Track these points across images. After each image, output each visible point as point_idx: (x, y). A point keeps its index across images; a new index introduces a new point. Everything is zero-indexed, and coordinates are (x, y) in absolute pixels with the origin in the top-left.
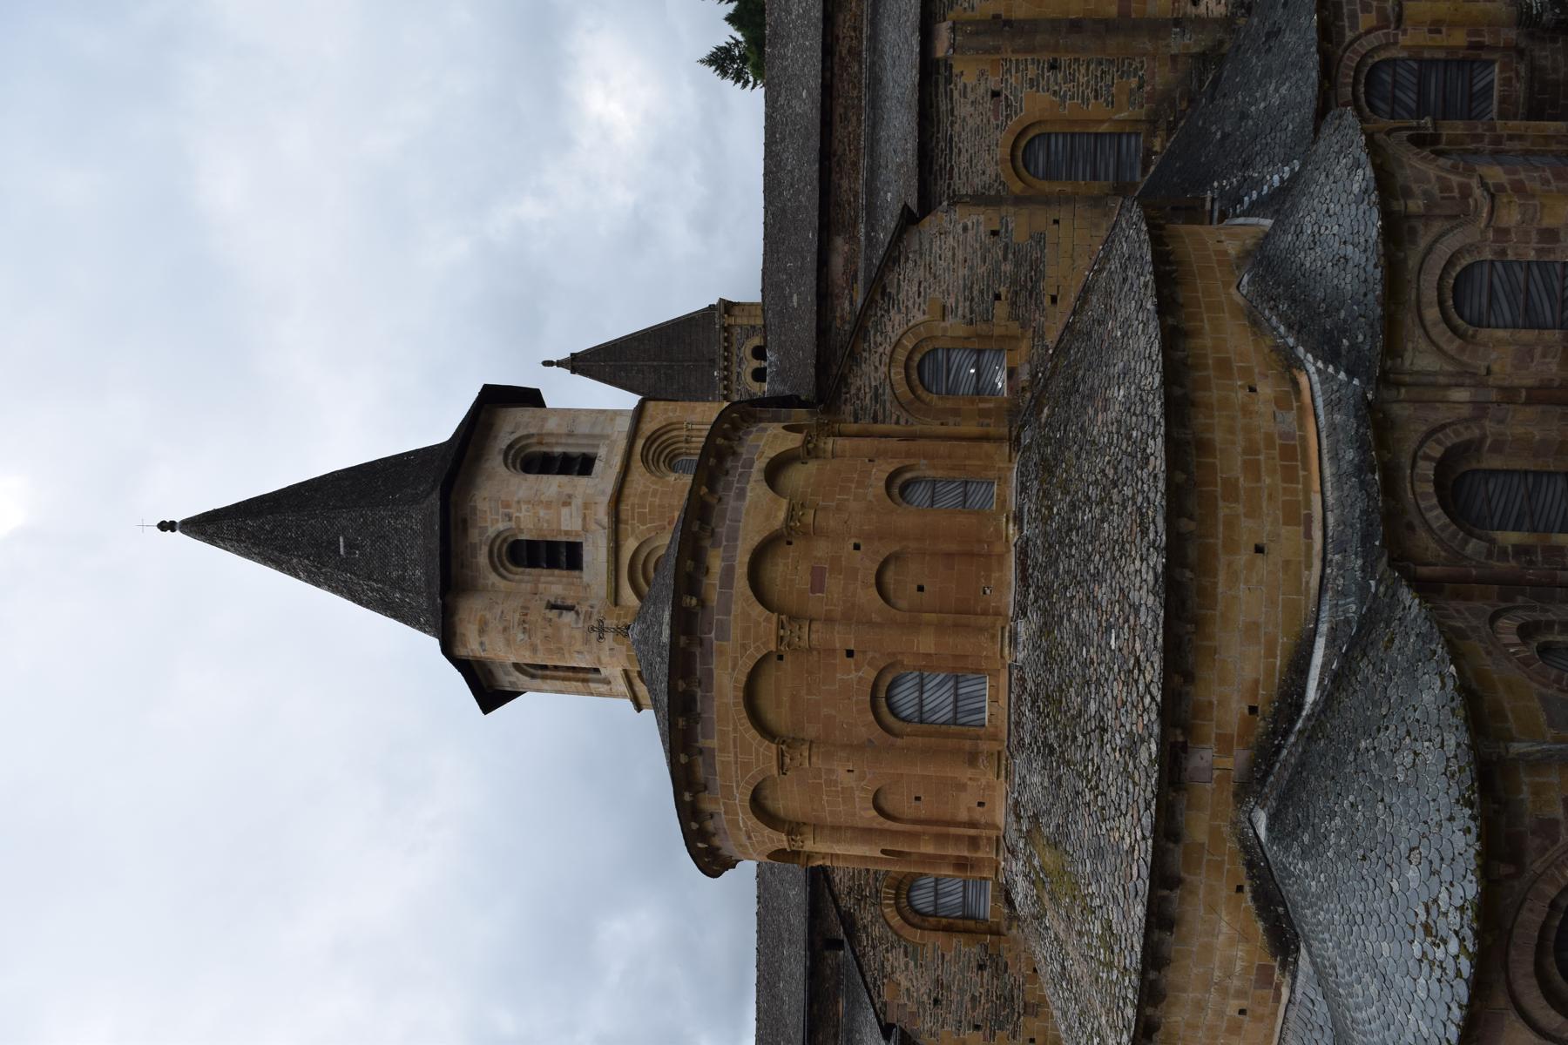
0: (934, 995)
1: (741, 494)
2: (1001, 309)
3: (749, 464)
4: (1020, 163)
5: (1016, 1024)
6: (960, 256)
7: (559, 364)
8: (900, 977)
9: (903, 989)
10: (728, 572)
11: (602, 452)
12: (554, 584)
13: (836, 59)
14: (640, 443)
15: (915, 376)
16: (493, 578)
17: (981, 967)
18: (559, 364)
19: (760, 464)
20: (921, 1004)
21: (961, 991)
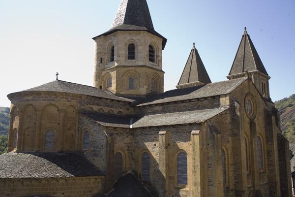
1: (44, 100)
2: (92, 148)
3: (52, 100)
4: (146, 151)
6: (100, 139)
7: (246, 31)
10: (28, 100)
11: (134, 60)
12: (107, 58)
13: (197, 102)
14: (133, 68)
15: (86, 130)
16: (107, 44)
18: (246, 31)
19: (53, 102)
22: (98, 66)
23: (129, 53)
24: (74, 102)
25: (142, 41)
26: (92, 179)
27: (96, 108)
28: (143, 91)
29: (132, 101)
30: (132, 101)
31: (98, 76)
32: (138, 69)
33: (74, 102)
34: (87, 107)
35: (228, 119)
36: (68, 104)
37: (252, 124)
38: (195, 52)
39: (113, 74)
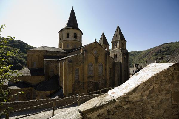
22: (59, 41)
23: (67, 36)
24: (42, 53)
25: (72, 32)
26: (40, 77)
27: (50, 54)
28: (70, 48)
29: (65, 51)
30: (65, 51)
31: (60, 44)
32: (69, 41)
33: (42, 53)
34: (47, 54)
35: (81, 57)
36: (39, 53)
37: (96, 59)
38: (103, 35)
39: (62, 43)
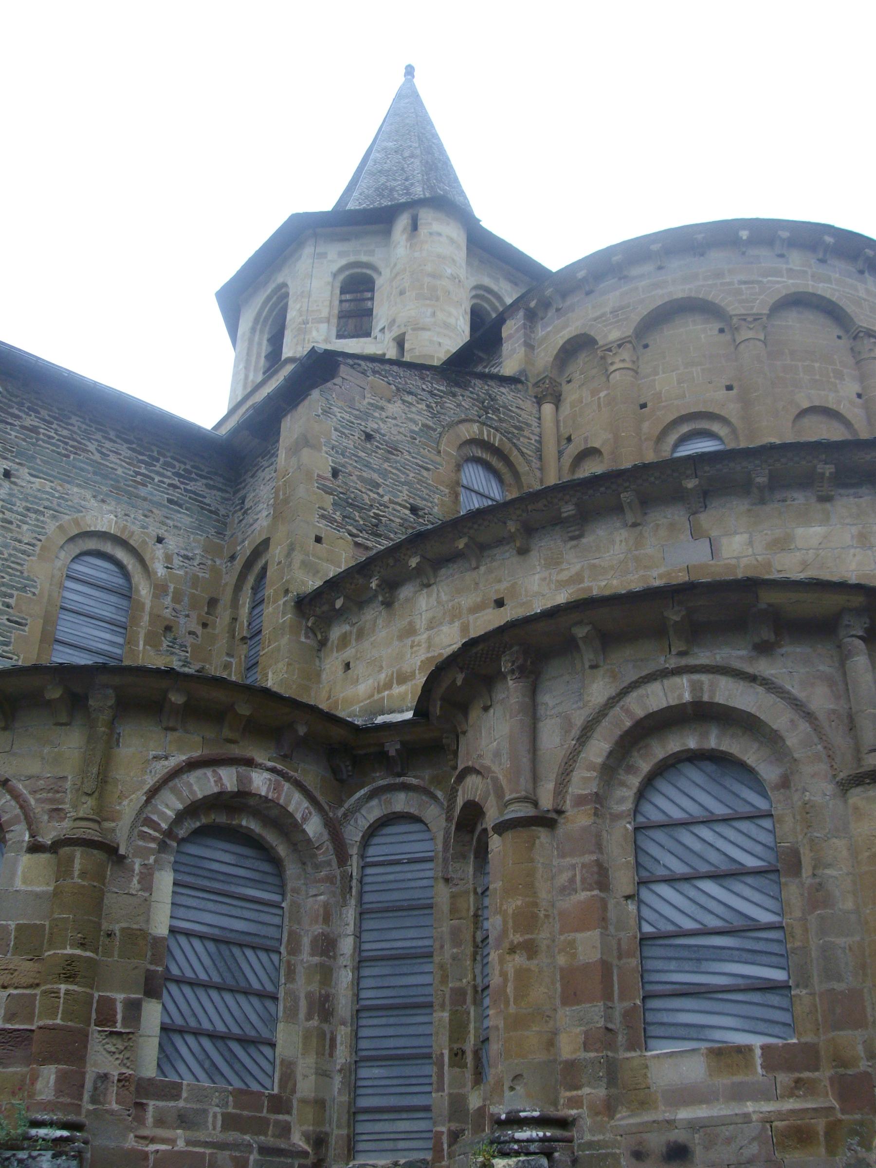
0: (377, 436)
5: (341, 526)
8: (395, 408)
9: (383, 403)
17: (414, 510)
20: (366, 415)
21: (384, 474)
